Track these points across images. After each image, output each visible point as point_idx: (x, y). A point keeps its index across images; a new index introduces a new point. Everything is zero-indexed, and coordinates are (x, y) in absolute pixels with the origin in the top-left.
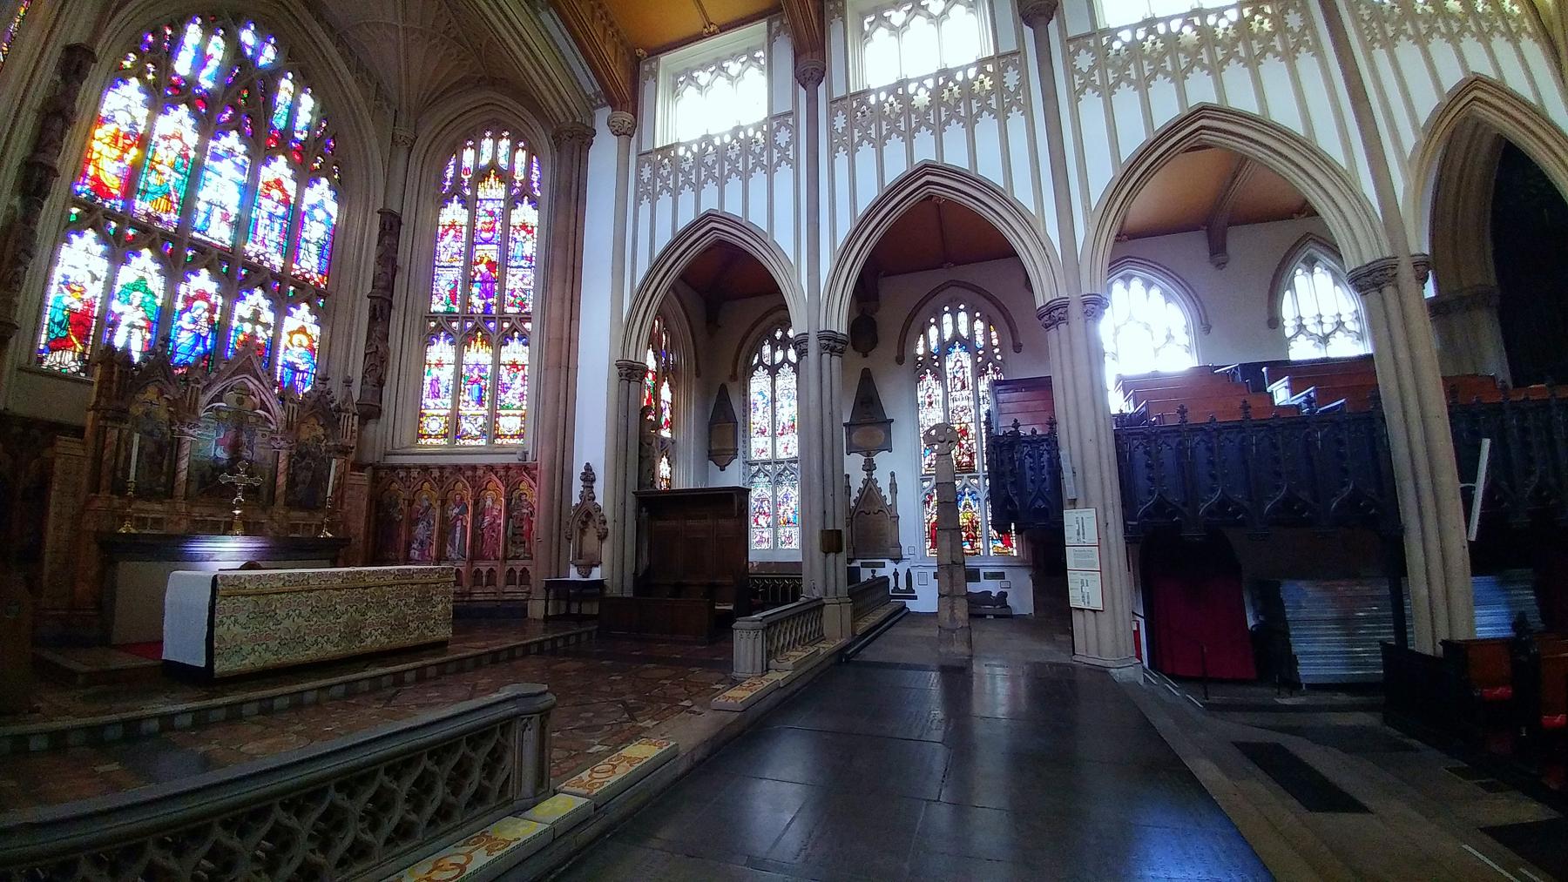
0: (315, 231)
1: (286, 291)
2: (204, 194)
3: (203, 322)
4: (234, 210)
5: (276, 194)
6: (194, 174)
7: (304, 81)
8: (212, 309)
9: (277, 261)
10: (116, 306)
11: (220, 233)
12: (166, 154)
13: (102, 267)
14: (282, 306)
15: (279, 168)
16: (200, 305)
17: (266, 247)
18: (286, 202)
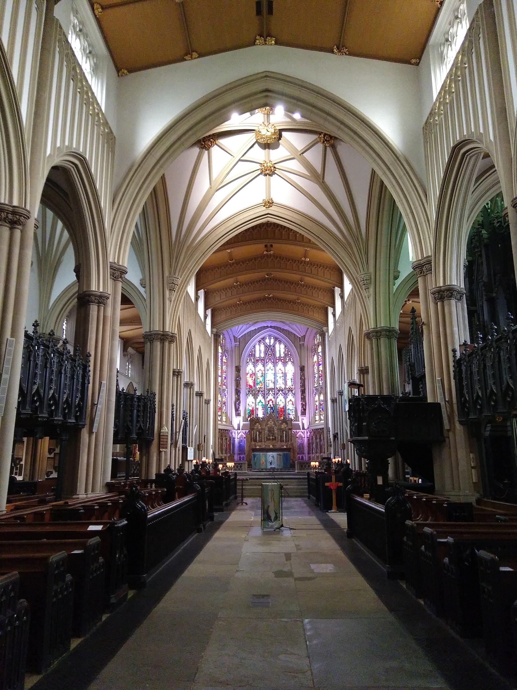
0: (290, 376)
1: (285, 392)
2: (267, 379)
3: (272, 406)
4: (273, 380)
5: (280, 372)
6: (264, 375)
7: (280, 342)
8: (273, 402)
9: (283, 387)
10: (257, 407)
11: (271, 386)
12: (259, 374)
13: (253, 400)
14: (285, 395)
15: (280, 365)
16: (271, 402)
17: (280, 384)
18: (282, 373)
